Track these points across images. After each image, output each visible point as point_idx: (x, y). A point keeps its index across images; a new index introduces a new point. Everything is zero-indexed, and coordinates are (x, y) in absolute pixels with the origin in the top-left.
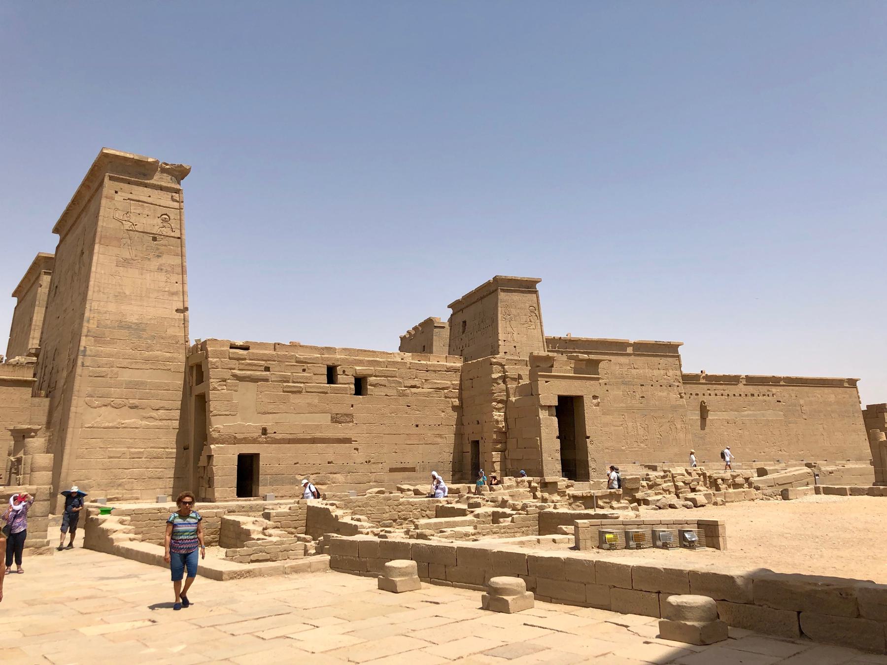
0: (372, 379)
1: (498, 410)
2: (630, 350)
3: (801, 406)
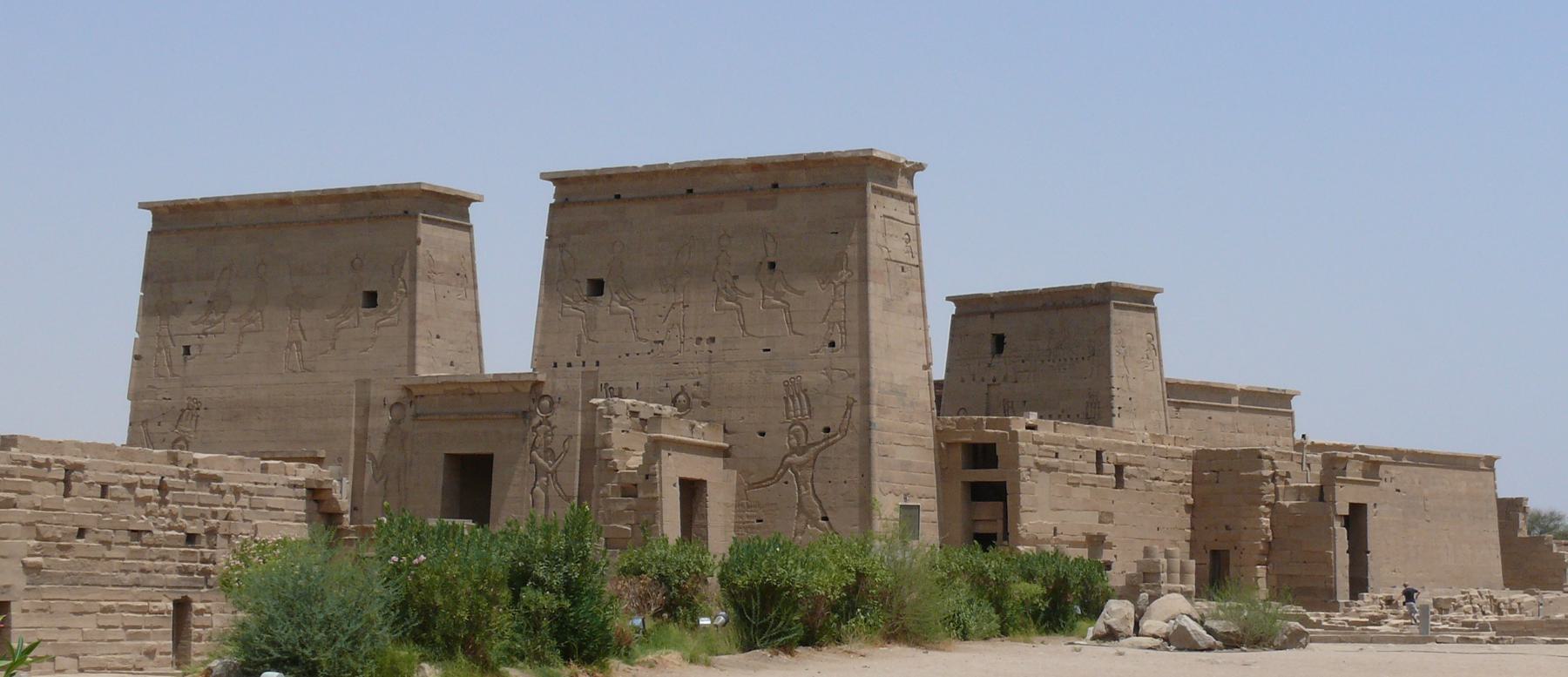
0: (1128, 469)
1: (1265, 515)
2: (1235, 402)
3: (1425, 499)
